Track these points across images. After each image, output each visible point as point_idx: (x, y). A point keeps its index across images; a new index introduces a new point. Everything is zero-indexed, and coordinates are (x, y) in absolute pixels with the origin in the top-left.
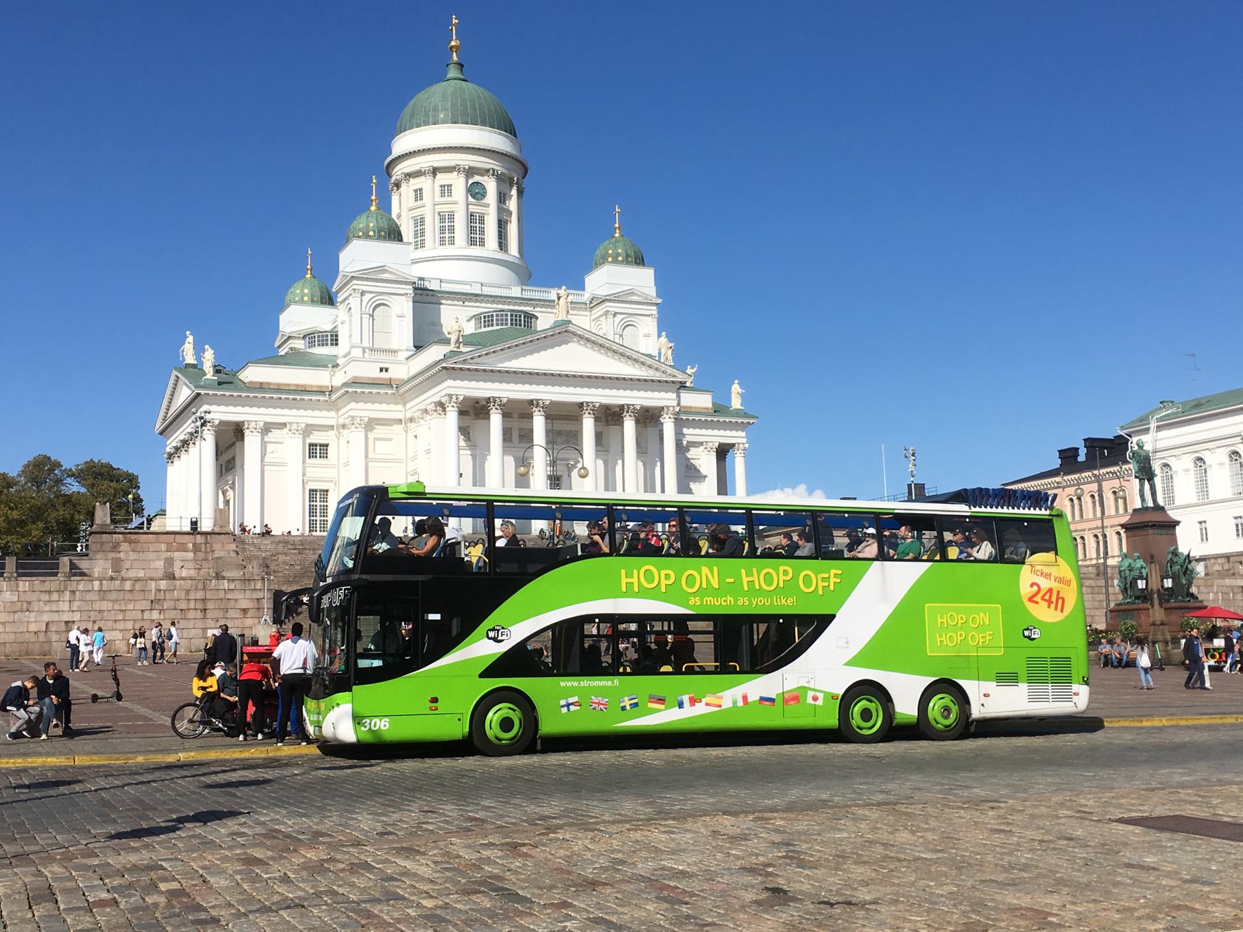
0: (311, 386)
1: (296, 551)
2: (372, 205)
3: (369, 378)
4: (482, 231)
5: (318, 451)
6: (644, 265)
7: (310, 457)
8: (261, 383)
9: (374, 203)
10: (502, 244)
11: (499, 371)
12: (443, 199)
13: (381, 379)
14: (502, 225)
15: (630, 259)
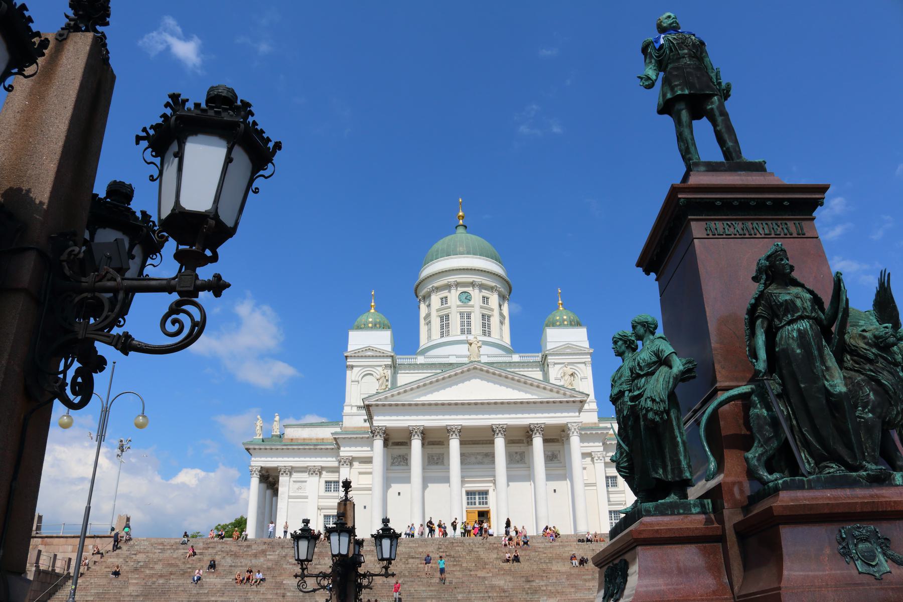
0: (327, 439)
1: (159, 551)
2: (371, 309)
3: (355, 428)
4: (469, 324)
5: (332, 487)
6: (580, 325)
7: (326, 491)
8: (292, 439)
9: (373, 308)
10: (486, 329)
11: (416, 405)
12: (442, 306)
13: (364, 427)
14: (486, 318)
15: (566, 323)
